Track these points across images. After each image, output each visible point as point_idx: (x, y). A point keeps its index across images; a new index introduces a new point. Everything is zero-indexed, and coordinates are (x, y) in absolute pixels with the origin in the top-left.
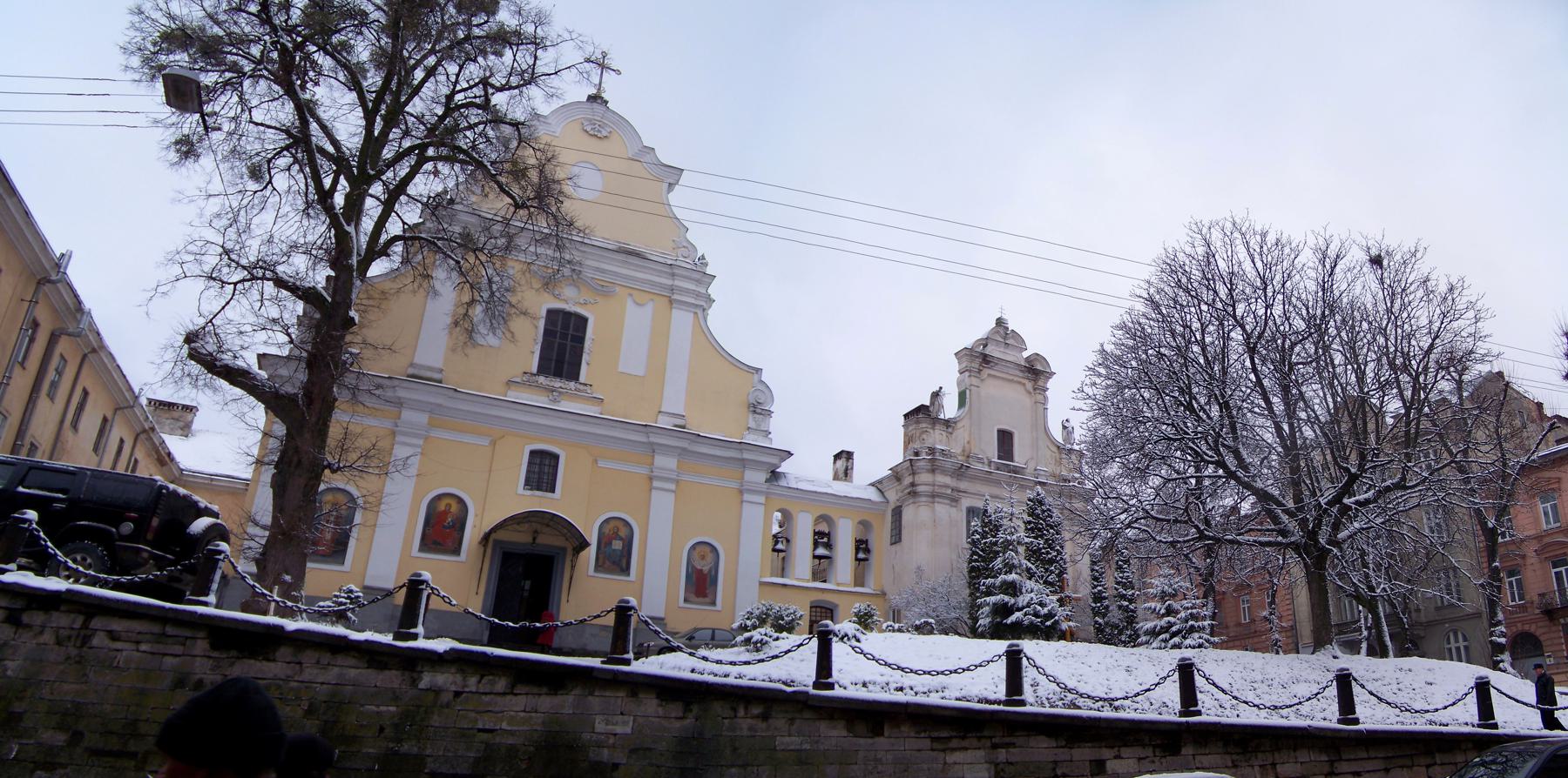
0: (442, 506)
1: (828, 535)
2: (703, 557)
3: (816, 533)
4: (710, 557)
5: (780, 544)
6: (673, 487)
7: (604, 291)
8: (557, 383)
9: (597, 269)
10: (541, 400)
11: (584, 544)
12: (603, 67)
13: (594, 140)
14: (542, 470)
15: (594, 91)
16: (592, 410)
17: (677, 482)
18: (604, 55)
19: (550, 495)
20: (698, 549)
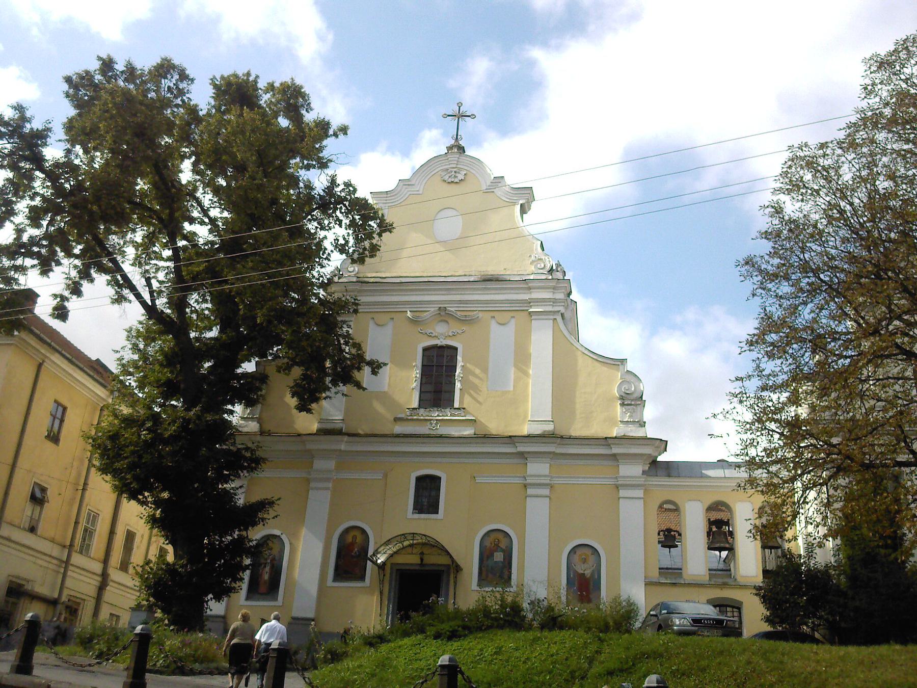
0: (349, 539)
2: (585, 561)
3: (711, 523)
4: (592, 559)
6: (546, 492)
7: (467, 321)
8: (435, 414)
9: (460, 302)
13: (453, 185)
15: (453, 142)
16: (468, 432)
17: (551, 487)
18: (460, 105)
20: (579, 552)
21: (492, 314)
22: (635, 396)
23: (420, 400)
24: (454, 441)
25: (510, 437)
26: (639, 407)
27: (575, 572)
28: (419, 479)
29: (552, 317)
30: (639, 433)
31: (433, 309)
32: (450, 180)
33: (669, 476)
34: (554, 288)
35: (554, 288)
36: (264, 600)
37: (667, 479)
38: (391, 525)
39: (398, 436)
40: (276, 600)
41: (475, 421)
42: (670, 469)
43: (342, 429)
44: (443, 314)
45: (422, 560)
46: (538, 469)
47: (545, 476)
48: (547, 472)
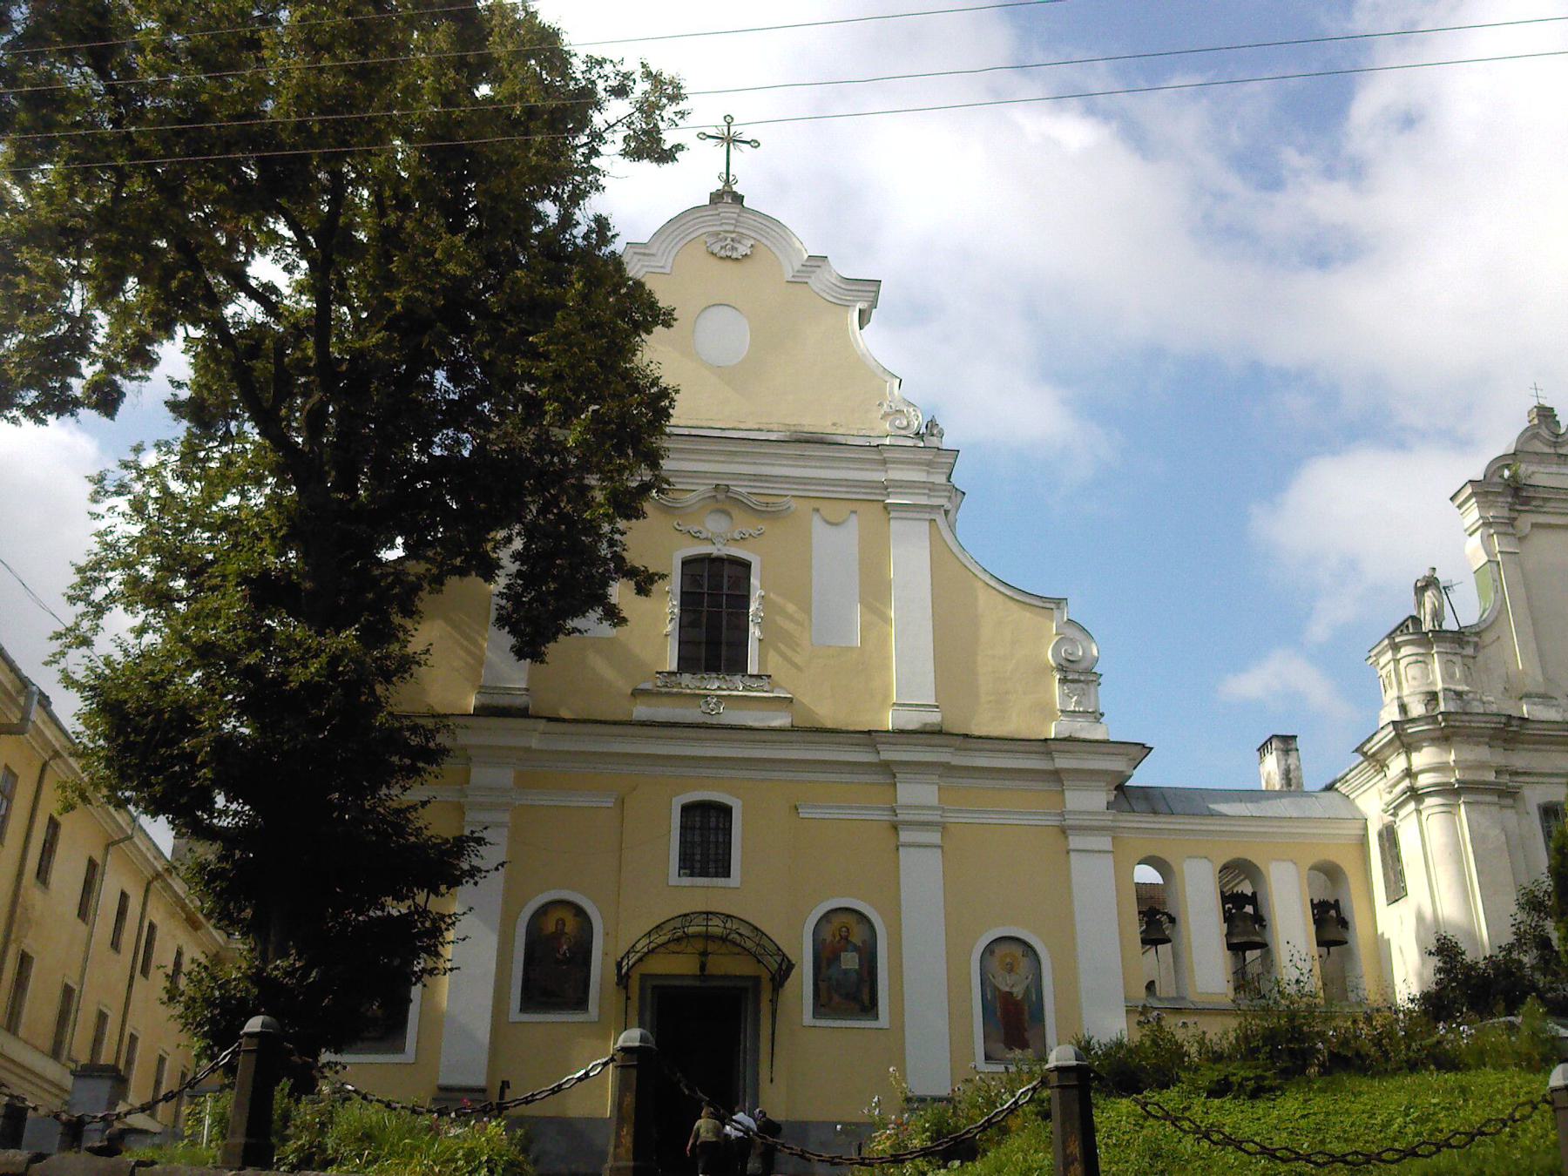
0: (551, 927)
1: (1253, 899)
2: (1011, 969)
3: (1225, 898)
4: (1024, 965)
5: (1156, 921)
6: (934, 837)
7: (768, 512)
8: (713, 685)
9: (757, 477)
10: (692, 714)
11: (785, 969)
12: (729, 140)
13: (730, 264)
14: (706, 838)
15: (720, 185)
16: (781, 720)
17: (943, 827)
18: (729, 120)
19: (720, 882)
20: (1001, 950)
21: (817, 504)
22: (1083, 665)
23: (681, 659)
24: (758, 736)
25: (869, 732)
26: (1092, 686)
27: (996, 988)
28: (687, 809)
29: (927, 516)
30: (1098, 733)
31: (703, 488)
32: (723, 253)
33: (1155, 812)
34: (929, 464)
35: (929, 464)
36: (377, 1052)
37: (1151, 818)
38: (637, 904)
39: (643, 724)
40: (402, 1050)
41: (791, 700)
42: (1152, 801)
43: (527, 709)
44: (723, 498)
45: (703, 967)
46: (916, 794)
47: (930, 808)
48: (935, 802)
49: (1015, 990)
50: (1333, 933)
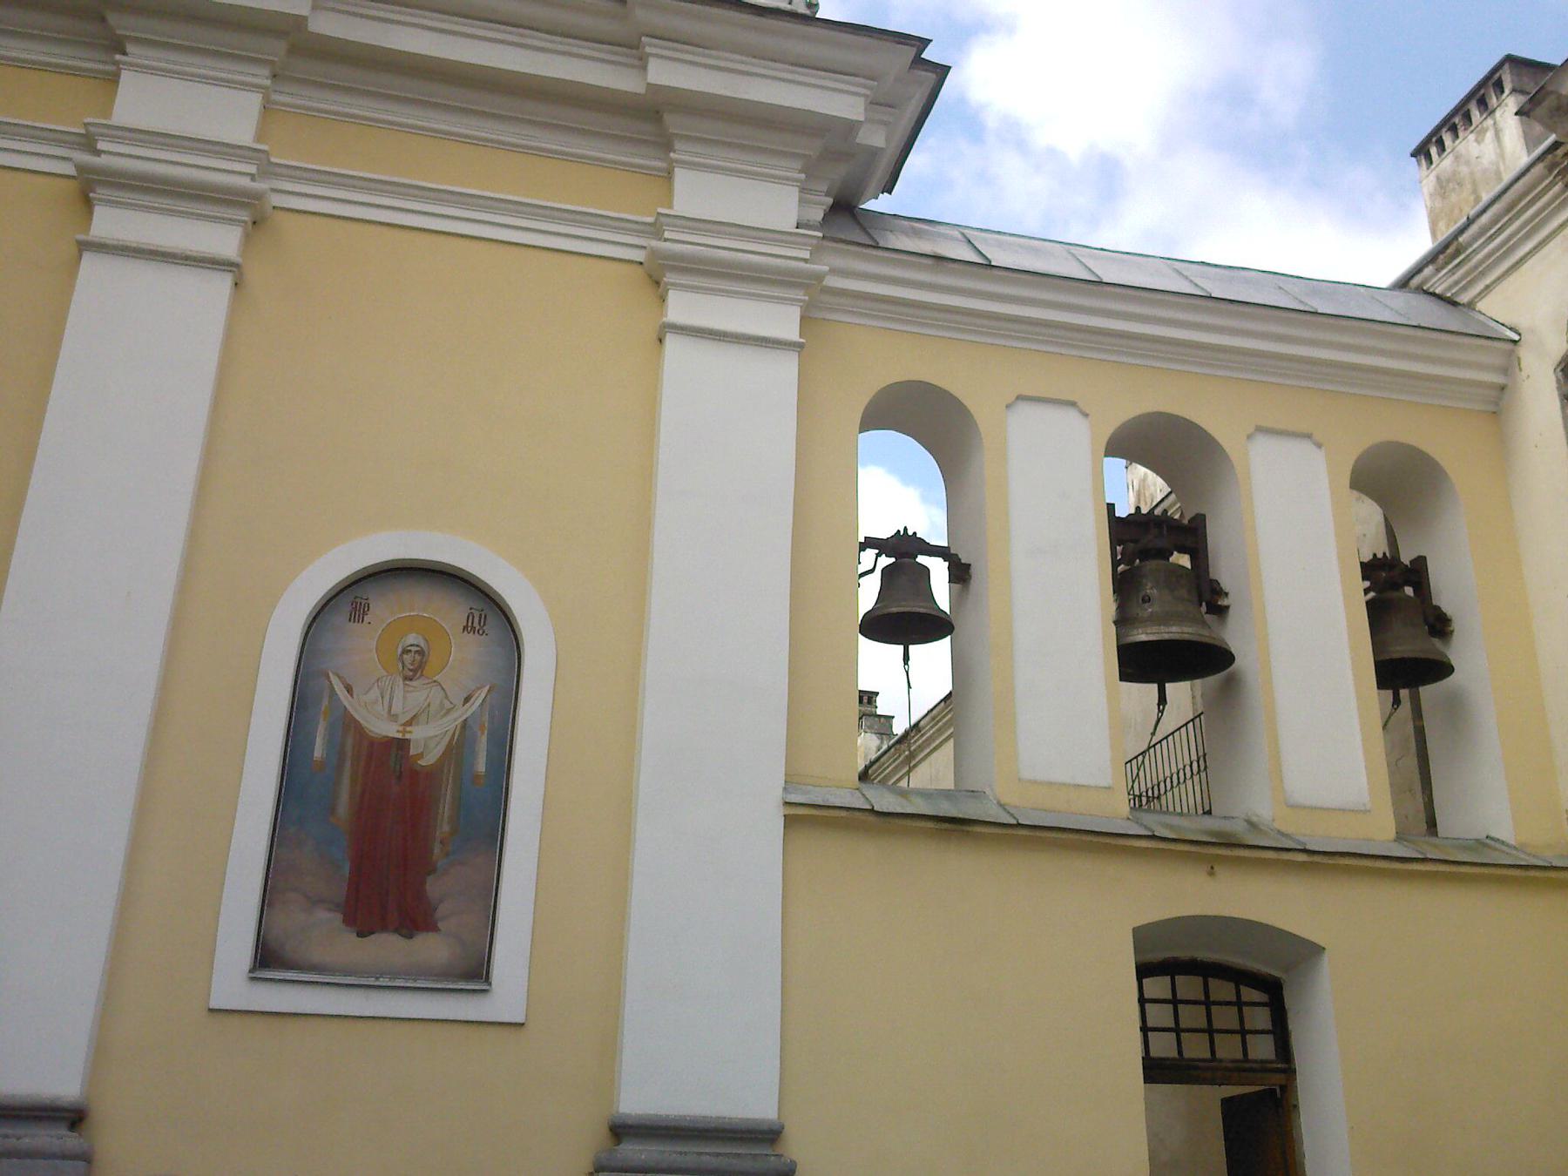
2: (415, 666)
4: (465, 658)
17: (256, 217)
20: (386, 608)
27: (348, 724)
49: (417, 734)
50: (1410, 644)
